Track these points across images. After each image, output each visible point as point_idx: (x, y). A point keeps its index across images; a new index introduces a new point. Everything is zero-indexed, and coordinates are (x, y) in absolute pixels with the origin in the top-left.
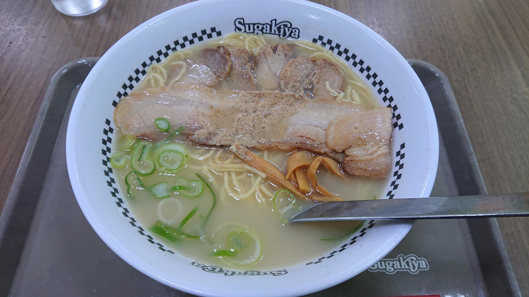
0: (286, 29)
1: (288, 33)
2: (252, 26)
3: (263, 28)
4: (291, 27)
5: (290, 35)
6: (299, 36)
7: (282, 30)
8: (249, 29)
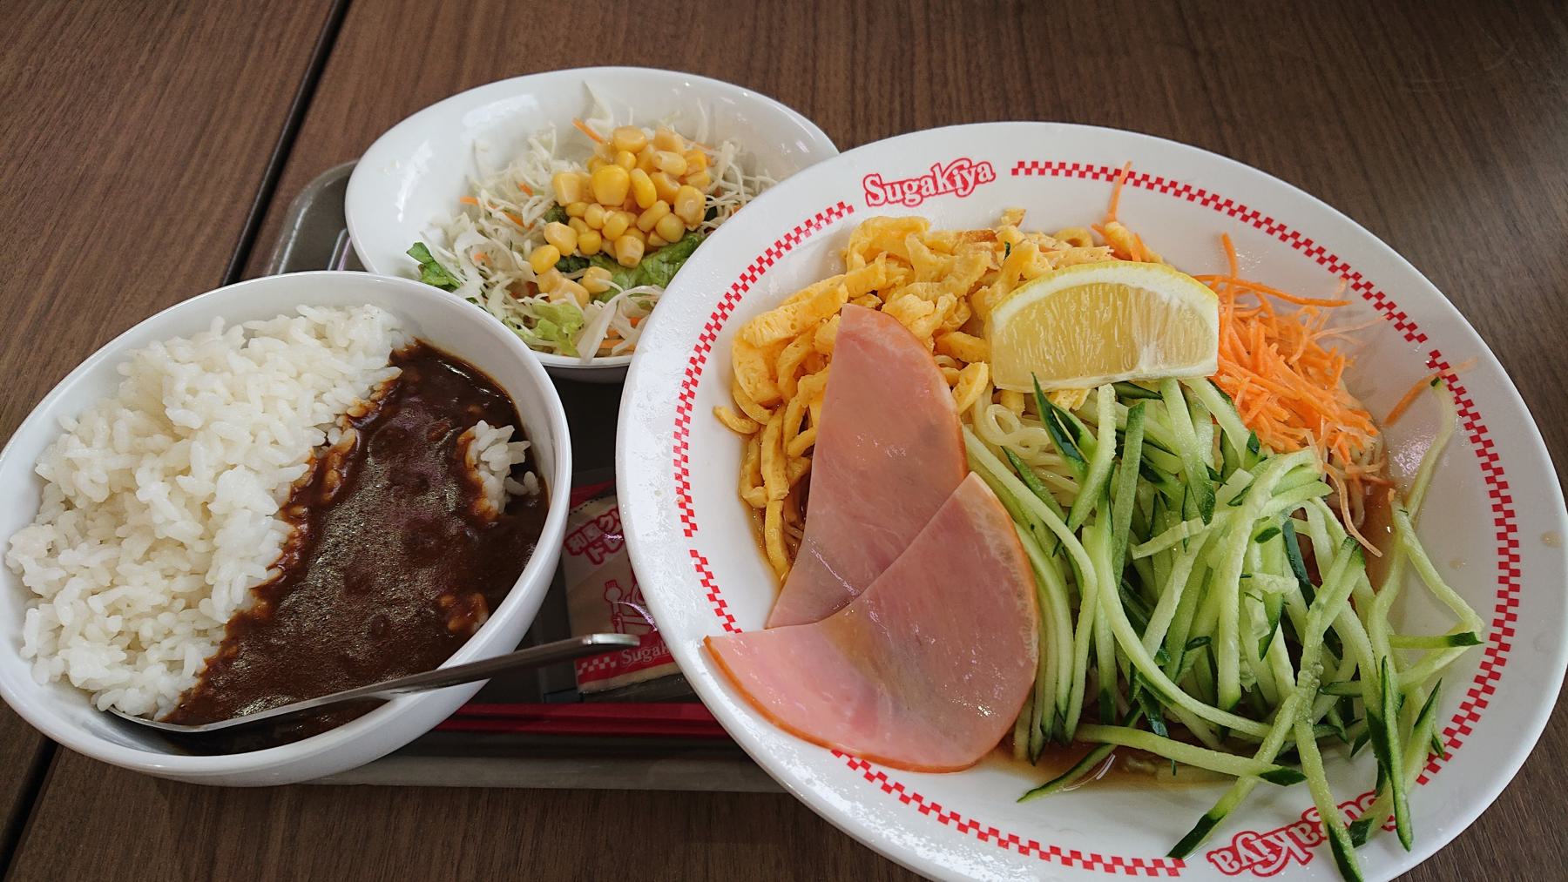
0: (965, 173)
1: (971, 180)
2: (897, 187)
3: (920, 187)
5: (977, 181)
6: (994, 174)
7: (958, 179)
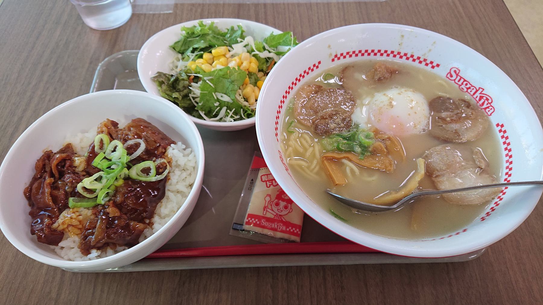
0: (486, 102)
2: (462, 80)
3: (469, 88)
4: (490, 103)
6: (491, 115)
7: (482, 101)
8: (459, 81)
